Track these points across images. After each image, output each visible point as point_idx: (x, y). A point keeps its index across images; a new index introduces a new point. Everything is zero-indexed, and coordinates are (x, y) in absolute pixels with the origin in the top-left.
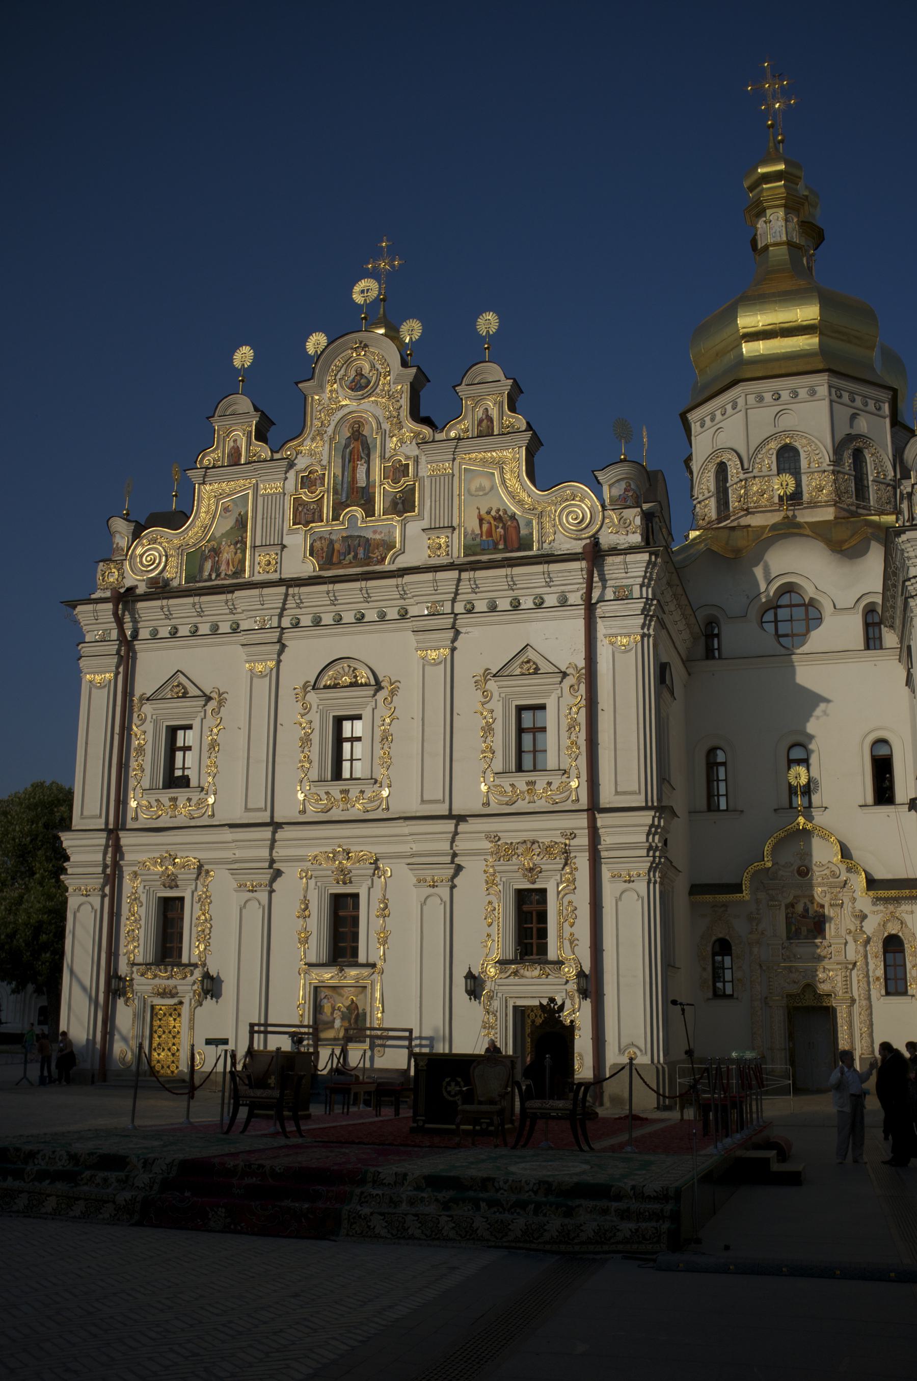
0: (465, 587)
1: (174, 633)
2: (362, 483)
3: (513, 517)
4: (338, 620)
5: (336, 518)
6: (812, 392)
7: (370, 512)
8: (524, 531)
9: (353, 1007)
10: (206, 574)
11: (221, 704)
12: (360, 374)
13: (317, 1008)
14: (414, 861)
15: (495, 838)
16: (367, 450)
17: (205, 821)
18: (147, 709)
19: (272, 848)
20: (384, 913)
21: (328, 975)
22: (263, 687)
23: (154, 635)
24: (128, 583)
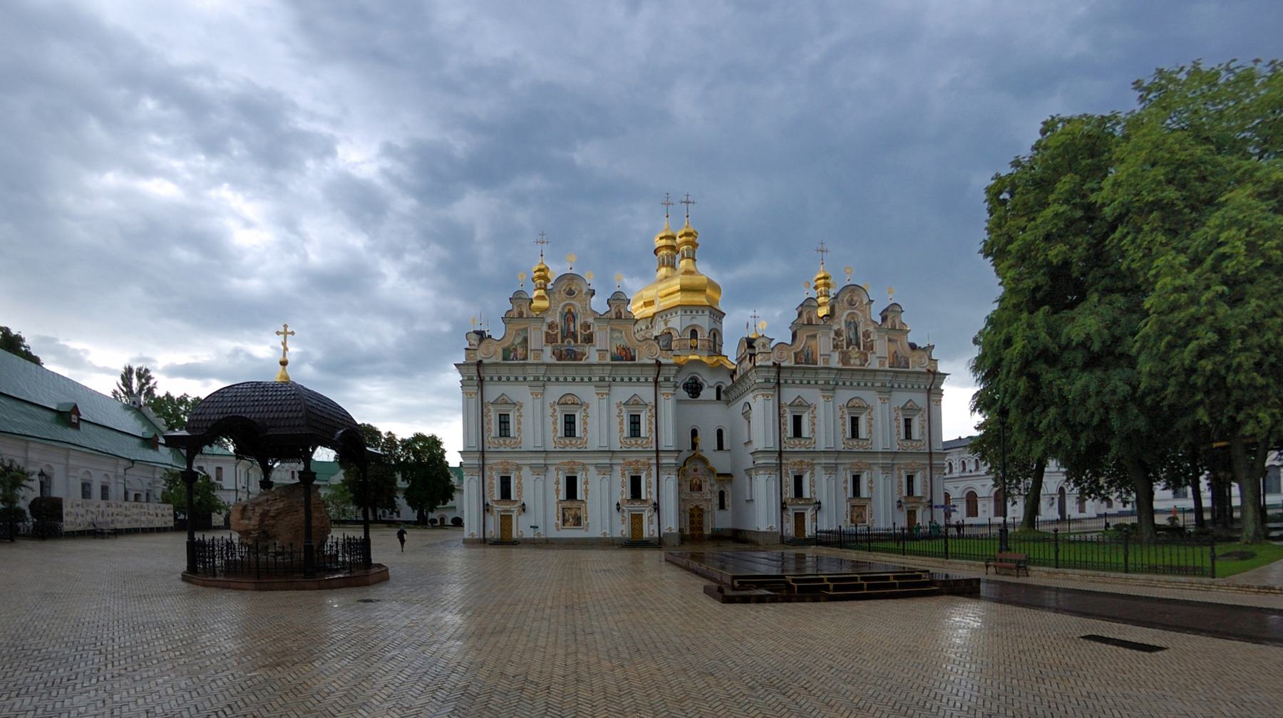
0: (614, 372)
1: (500, 379)
2: (572, 330)
3: (629, 349)
4: (565, 379)
5: (563, 342)
8: (632, 354)
9: (576, 514)
10: (511, 358)
11: (521, 406)
12: (570, 289)
13: (564, 515)
14: (596, 466)
15: (624, 460)
16: (574, 318)
17: (518, 449)
18: (491, 407)
19: (545, 460)
20: (586, 483)
21: (568, 504)
22: (538, 402)
23: (492, 379)
24: (479, 359)
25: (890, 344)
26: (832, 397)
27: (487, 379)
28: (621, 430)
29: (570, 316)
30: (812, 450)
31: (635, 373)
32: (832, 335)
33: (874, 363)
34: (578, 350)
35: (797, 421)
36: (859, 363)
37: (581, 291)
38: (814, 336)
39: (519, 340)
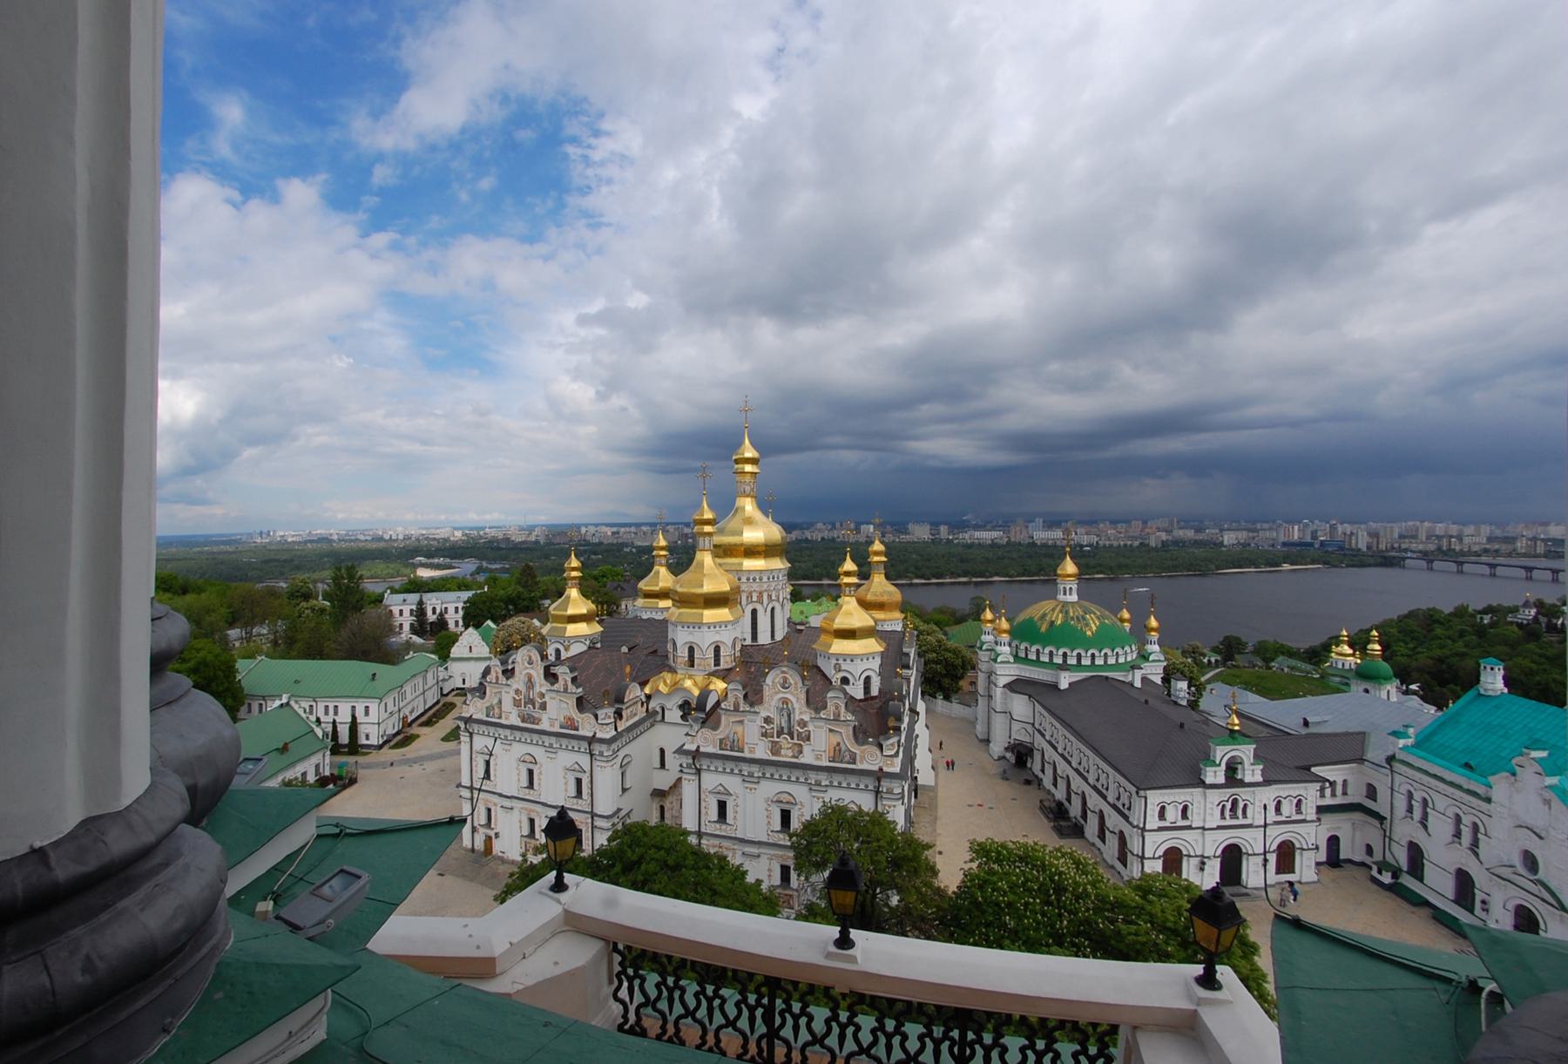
2: (531, 697)
5: (525, 707)
6: (699, 628)
7: (534, 708)
25: (831, 734)
26: (755, 789)
27: (476, 731)
28: (566, 790)
29: (530, 683)
30: (733, 835)
31: (575, 743)
32: (759, 721)
33: (807, 758)
34: (536, 715)
35: (722, 806)
36: (791, 754)
37: (537, 661)
38: (741, 722)
39: (495, 701)
